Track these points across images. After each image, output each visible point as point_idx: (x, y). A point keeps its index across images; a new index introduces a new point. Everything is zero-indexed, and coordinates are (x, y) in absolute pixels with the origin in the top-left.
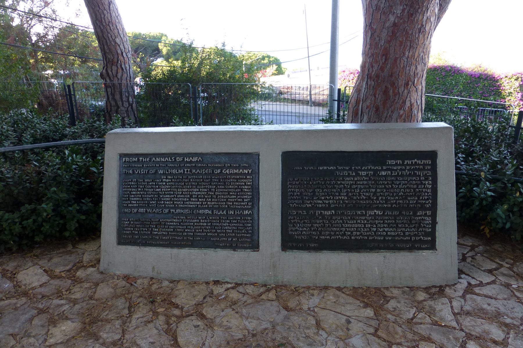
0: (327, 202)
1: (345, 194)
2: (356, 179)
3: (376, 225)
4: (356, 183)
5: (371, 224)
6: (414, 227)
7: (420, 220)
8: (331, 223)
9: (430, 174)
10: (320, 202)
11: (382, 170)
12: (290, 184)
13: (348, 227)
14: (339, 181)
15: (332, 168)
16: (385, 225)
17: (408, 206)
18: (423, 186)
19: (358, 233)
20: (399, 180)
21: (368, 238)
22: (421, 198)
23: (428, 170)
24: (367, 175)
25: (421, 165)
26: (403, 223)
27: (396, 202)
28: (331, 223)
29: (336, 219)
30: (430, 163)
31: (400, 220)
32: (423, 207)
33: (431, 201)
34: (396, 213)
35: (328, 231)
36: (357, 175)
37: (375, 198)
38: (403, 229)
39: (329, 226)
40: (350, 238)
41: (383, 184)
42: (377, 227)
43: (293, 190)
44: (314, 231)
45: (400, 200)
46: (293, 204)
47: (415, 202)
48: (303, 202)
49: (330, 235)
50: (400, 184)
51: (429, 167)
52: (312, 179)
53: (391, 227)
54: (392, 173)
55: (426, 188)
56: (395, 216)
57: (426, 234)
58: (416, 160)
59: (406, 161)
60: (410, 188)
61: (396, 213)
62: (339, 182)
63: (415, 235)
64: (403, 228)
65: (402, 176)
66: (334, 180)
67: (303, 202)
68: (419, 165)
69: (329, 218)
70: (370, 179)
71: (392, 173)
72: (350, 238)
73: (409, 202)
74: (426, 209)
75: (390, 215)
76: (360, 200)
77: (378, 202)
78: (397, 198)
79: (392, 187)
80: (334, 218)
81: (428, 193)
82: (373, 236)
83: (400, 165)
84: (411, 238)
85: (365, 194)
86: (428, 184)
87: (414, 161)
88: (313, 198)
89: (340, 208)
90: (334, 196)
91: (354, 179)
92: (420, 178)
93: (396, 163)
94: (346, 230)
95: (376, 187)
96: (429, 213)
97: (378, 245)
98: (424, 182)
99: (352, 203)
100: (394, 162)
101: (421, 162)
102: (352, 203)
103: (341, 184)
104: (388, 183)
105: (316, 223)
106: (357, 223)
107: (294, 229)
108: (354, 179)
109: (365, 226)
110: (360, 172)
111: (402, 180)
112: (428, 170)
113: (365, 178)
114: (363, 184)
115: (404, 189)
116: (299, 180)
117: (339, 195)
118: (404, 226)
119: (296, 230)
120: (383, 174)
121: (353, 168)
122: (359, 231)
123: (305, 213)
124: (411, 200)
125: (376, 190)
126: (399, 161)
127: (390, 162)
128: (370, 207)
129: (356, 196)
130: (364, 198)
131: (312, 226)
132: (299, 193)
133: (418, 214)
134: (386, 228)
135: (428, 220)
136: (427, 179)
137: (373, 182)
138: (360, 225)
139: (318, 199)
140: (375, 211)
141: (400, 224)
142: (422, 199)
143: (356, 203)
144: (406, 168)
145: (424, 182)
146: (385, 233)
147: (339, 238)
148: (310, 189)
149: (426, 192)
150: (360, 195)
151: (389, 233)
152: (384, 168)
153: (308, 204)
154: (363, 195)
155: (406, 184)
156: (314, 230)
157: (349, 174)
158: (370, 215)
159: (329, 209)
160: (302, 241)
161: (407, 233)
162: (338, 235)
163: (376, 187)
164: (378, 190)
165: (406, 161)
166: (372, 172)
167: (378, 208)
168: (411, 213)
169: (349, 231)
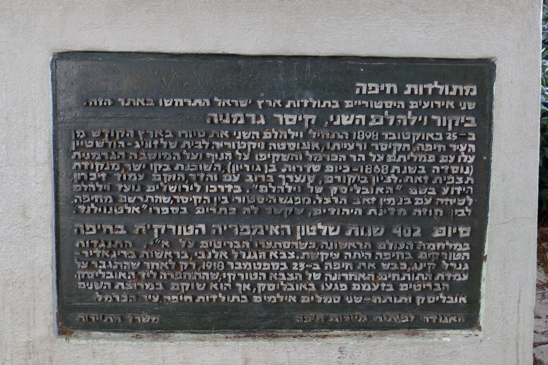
0: (185, 199)
1: (236, 179)
2: (267, 135)
3: (322, 266)
4: (267, 146)
5: (307, 261)
6: (424, 270)
7: (441, 250)
8: (194, 258)
9: (473, 124)
10: (165, 199)
11: (342, 109)
12: (77, 149)
13: (243, 271)
14: (219, 140)
15: (198, 101)
16: (347, 265)
17: (409, 213)
18: (452, 159)
19: (271, 287)
20: (388, 141)
21: (298, 299)
22: (445, 191)
23: (467, 112)
24: (300, 123)
25: (450, 97)
26: (393, 259)
27: (377, 202)
28: (194, 258)
29: (211, 248)
30: (474, 93)
31: (387, 250)
32: (449, 217)
33: (471, 201)
34: (377, 231)
35: (187, 280)
36: (271, 123)
37: (319, 190)
38: (394, 276)
39: (190, 266)
40: (250, 299)
41: (343, 150)
42: (322, 271)
43: (86, 164)
44: (147, 279)
45: (390, 195)
46: (88, 204)
47: (428, 202)
48: (115, 199)
49: (195, 293)
50: (390, 151)
51: (471, 106)
52: (140, 133)
53: (362, 270)
54: (368, 120)
55: (459, 165)
56: (374, 241)
57: (454, 289)
58: (436, 85)
59: (409, 87)
60: (418, 163)
61: (377, 231)
62: (219, 145)
63: (425, 292)
64: (396, 271)
65: (397, 127)
66: (206, 137)
67: (115, 199)
68: (444, 97)
69: (191, 245)
70: (307, 137)
71: (368, 120)
72: (250, 299)
73: (413, 201)
74: (457, 221)
75: (360, 238)
76: (278, 194)
77: (328, 201)
78: (381, 190)
79: (368, 158)
80: (204, 244)
81: (465, 177)
82: (312, 294)
83: (392, 96)
84: (414, 300)
85: (291, 177)
86: (466, 152)
87: (430, 87)
88: (143, 189)
89: (222, 218)
90: (204, 183)
91: (261, 135)
92: (444, 136)
93: (382, 92)
94: (238, 278)
95: (324, 159)
96: (464, 231)
97: (326, 319)
98: (455, 147)
99: (255, 204)
100: (375, 88)
101: (451, 89)
102: (255, 204)
103: (225, 148)
104: (356, 148)
105: (154, 259)
106: (267, 259)
107: (91, 274)
108: (261, 135)
109: (290, 265)
110: (280, 116)
111: (397, 140)
112: (467, 112)
113: (294, 134)
114: (287, 151)
115: (401, 165)
116: (102, 134)
117: (220, 181)
118: (396, 267)
119: (98, 278)
120: (345, 122)
121: (260, 103)
122: (274, 281)
123: (123, 232)
124: (418, 195)
125: (323, 168)
126: (388, 86)
127: (363, 87)
128: (307, 217)
129: (266, 183)
130: (290, 188)
131: (142, 267)
132: (104, 175)
133: (437, 235)
134: (349, 271)
135: (462, 251)
136: (462, 139)
137: (316, 145)
138: (275, 265)
139: (159, 191)
140: (320, 226)
141: (386, 262)
142: (448, 195)
143: (266, 203)
144: (407, 105)
145: (455, 147)
146: (344, 287)
147: (218, 299)
148: (137, 162)
149: (459, 174)
150: (277, 182)
151: (356, 287)
152: (348, 104)
153: (130, 205)
154: (287, 180)
155: (406, 152)
156: (148, 279)
157: (247, 120)
158: (304, 238)
159: (190, 218)
160: (115, 308)
161: (404, 287)
162: (214, 291)
163: (324, 159)
164: (330, 168)
165: (409, 87)
166: (314, 117)
167: (325, 218)
168: (417, 233)
169: (246, 281)
